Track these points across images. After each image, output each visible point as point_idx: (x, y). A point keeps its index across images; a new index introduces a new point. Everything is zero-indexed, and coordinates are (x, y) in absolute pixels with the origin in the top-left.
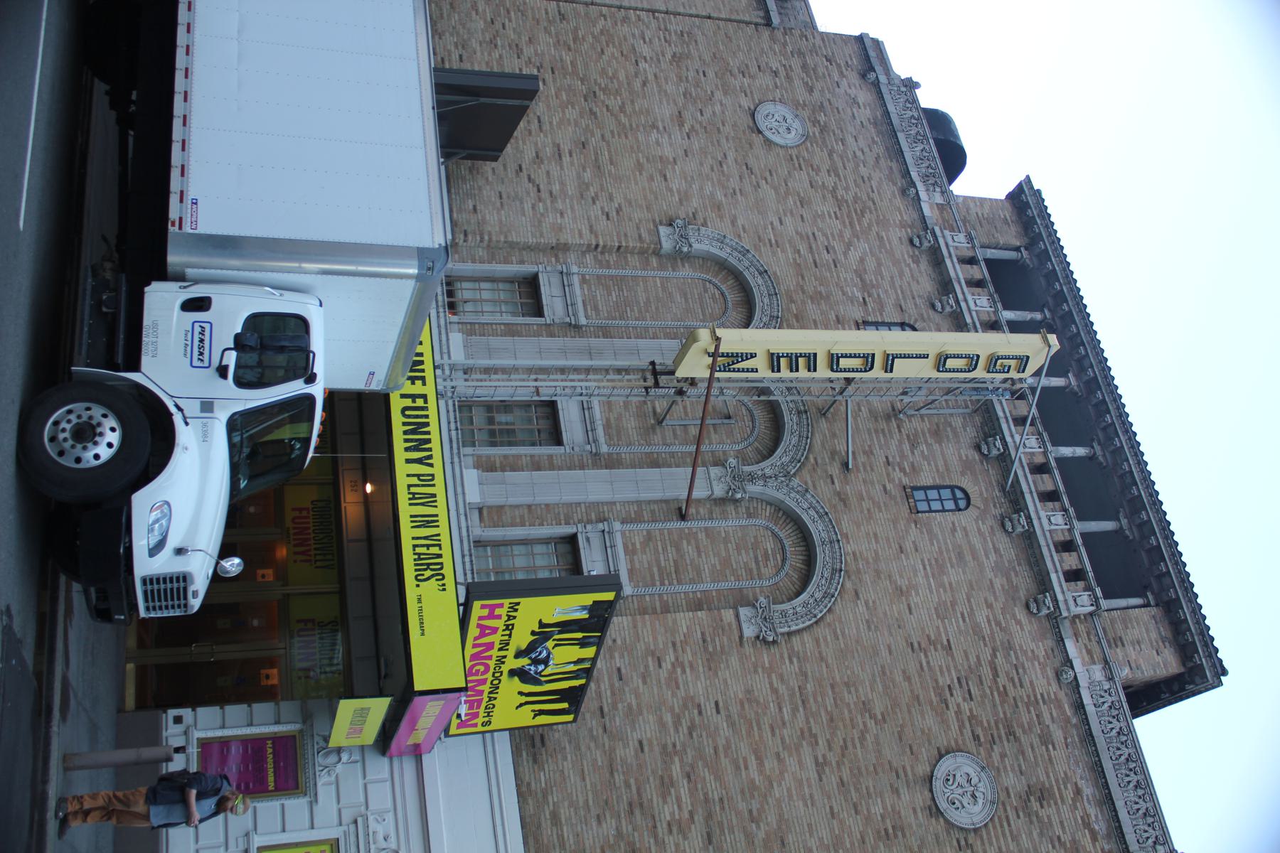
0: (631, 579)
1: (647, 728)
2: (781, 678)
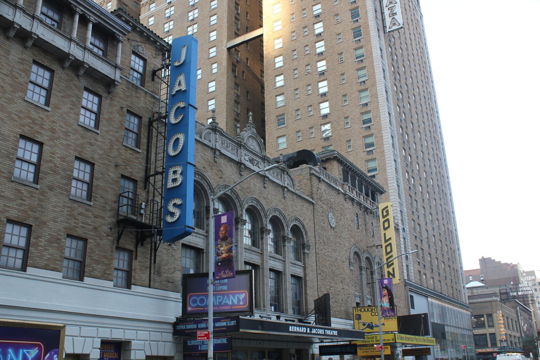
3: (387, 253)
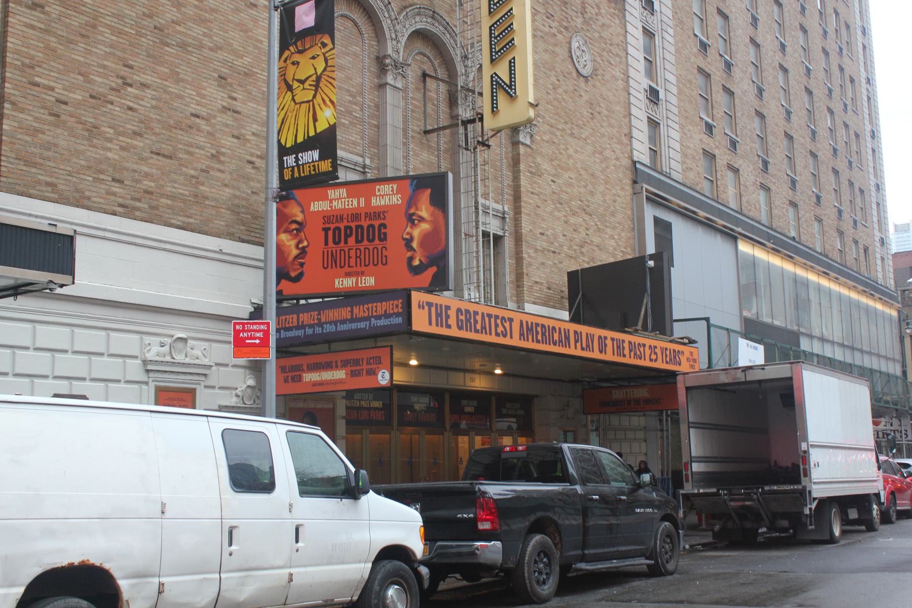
0: (498, 203)
1: (559, 230)
2: (545, 133)
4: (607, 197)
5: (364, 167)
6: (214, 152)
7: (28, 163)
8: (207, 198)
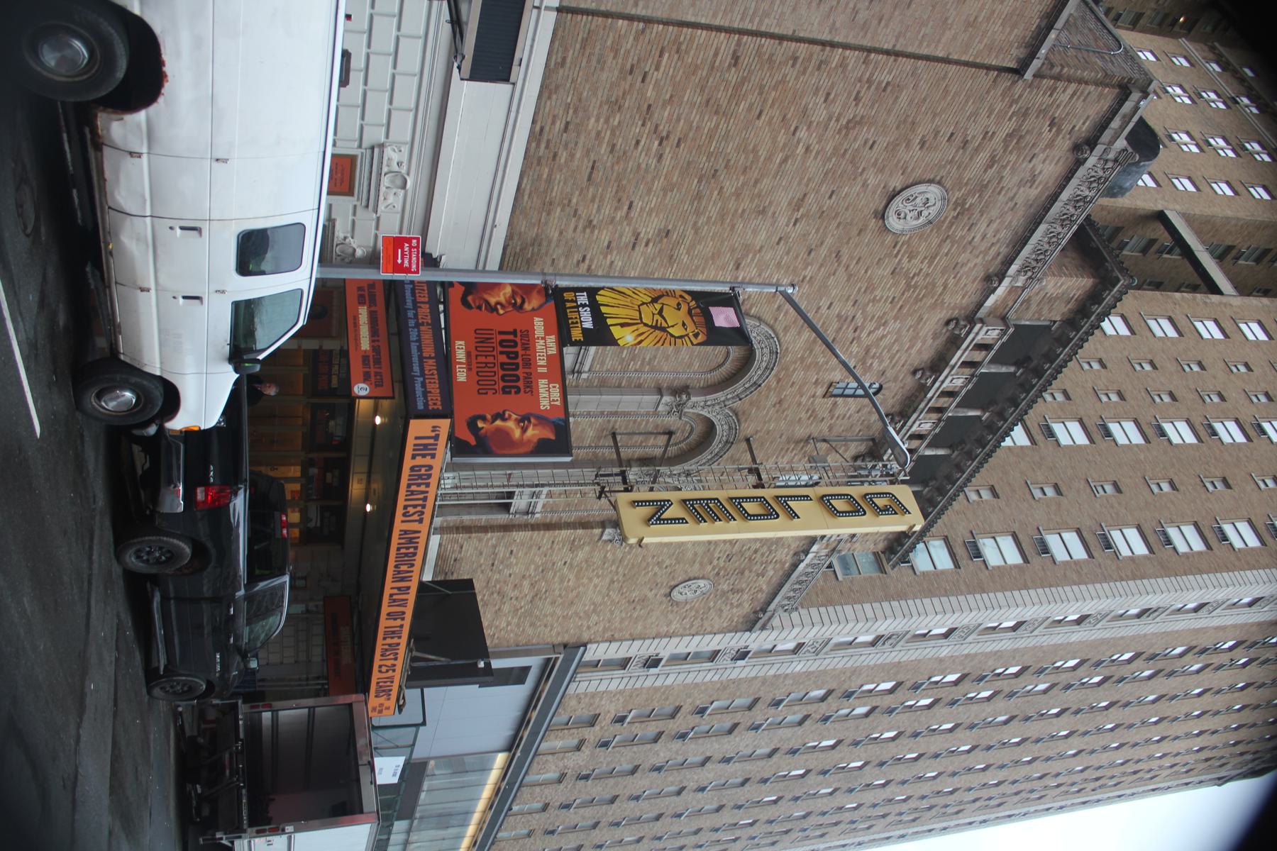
2: (614, 554)
3: (737, 502)
4: (549, 619)
5: (579, 372)
6: (595, 222)
7: (585, 42)
8: (549, 214)
